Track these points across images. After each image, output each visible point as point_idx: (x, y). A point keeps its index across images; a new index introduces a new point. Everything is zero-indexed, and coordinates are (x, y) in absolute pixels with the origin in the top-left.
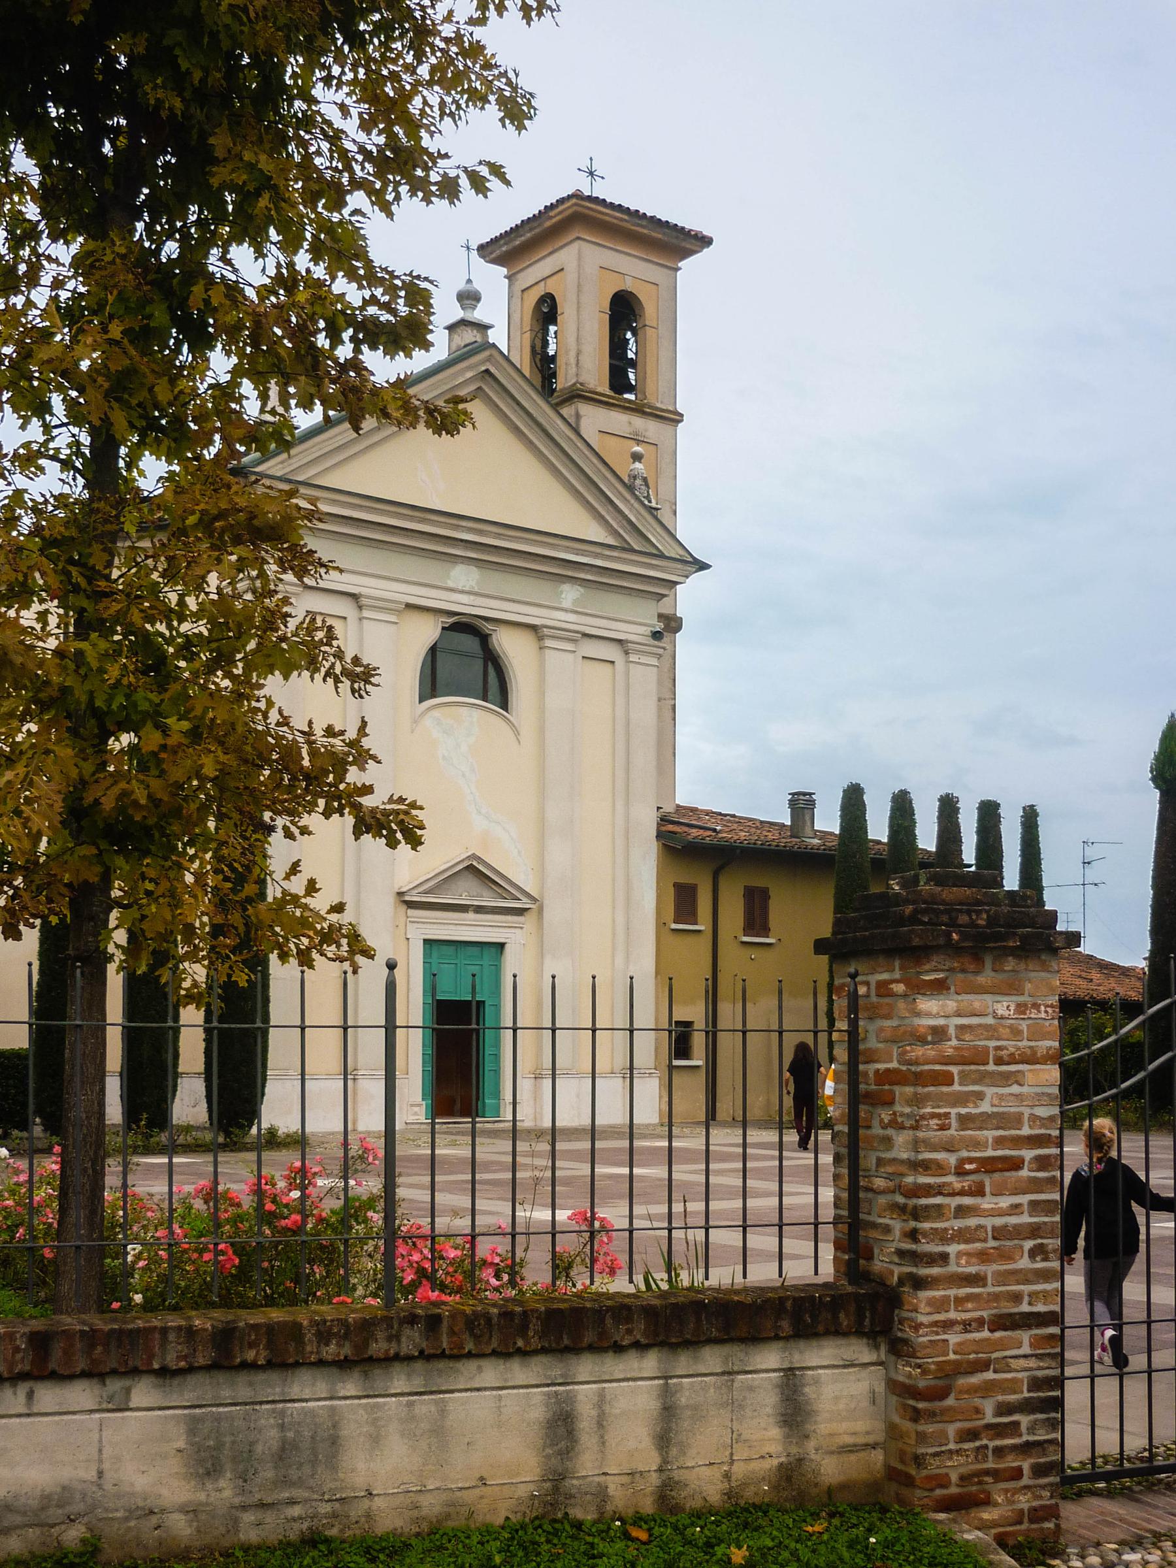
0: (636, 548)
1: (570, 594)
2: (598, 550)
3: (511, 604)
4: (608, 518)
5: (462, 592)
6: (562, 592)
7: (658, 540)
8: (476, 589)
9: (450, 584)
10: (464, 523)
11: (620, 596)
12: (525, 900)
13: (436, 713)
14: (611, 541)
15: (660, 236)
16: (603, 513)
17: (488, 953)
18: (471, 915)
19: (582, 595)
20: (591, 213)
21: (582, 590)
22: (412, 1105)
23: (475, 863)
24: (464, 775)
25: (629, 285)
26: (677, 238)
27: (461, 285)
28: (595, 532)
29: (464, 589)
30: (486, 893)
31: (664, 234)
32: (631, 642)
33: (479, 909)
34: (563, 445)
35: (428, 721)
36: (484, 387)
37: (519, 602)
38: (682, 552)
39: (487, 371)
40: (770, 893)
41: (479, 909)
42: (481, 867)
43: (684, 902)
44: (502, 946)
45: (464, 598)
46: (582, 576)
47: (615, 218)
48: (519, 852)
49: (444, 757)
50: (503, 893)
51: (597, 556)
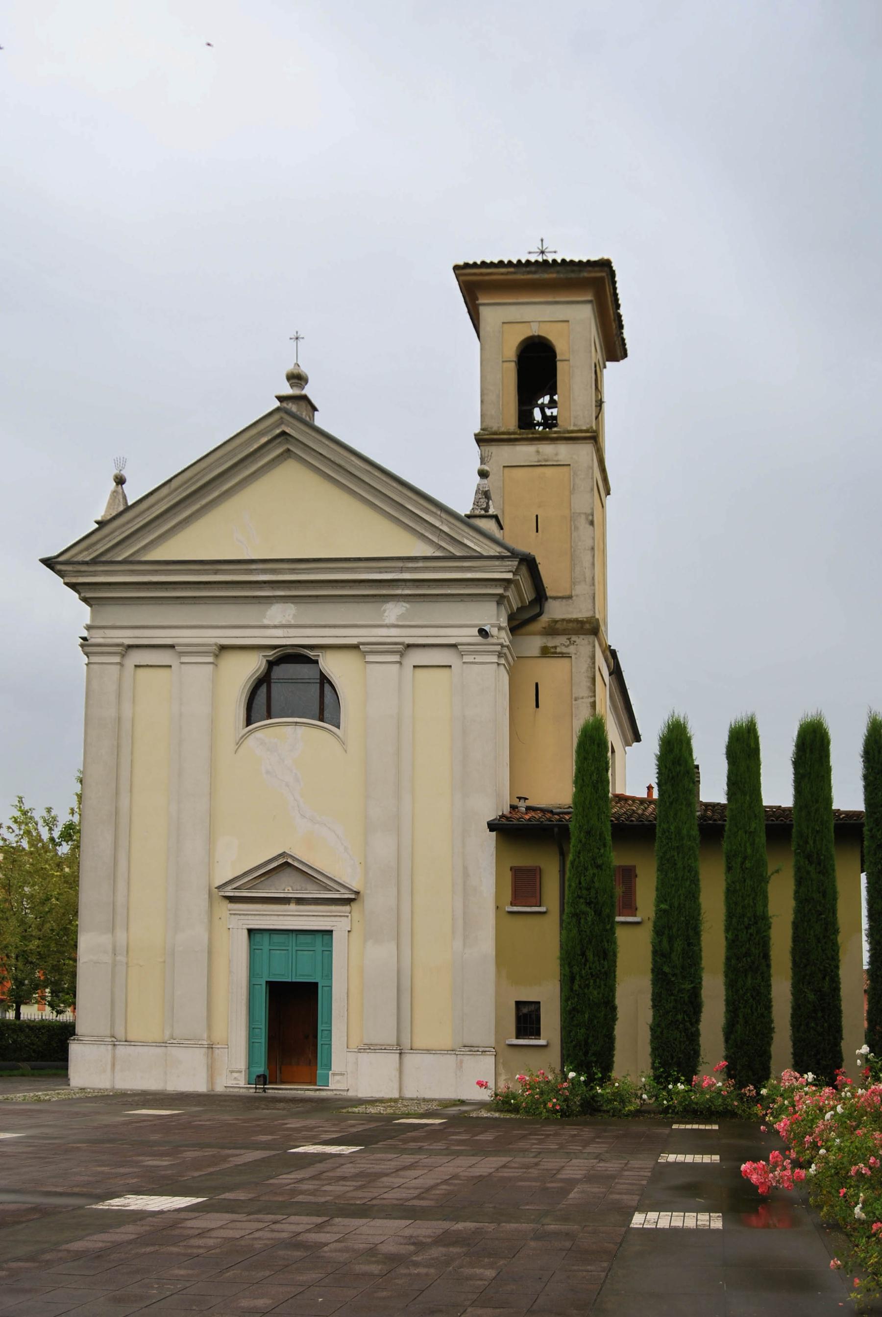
0: (458, 554)
1: (393, 612)
2: (400, 564)
3: (327, 630)
4: (427, 534)
5: (275, 627)
6: (385, 611)
7: (475, 544)
8: (293, 622)
9: (266, 622)
10: (254, 567)
11: (447, 604)
12: (343, 891)
13: (258, 734)
14: (438, 554)
15: (554, 276)
16: (423, 532)
17: (319, 939)
18: (293, 907)
19: (407, 609)
20: (487, 278)
21: (407, 605)
22: (232, 1072)
23: (290, 861)
24: (287, 785)
25: (535, 330)
26: (573, 271)
27: (290, 367)
28: (422, 549)
29: (282, 624)
30: (310, 886)
31: (558, 272)
32: (363, 644)
33: (300, 901)
34: (367, 480)
35: (251, 741)
36: (292, 448)
37: (335, 626)
38: (499, 549)
39: (284, 433)
40: (638, 872)
41: (300, 901)
42: (296, 864)
43: (523, 887)
44: (330, 932)
45: (279, 632)
46: (399, 592)
47: (502, 274)
48: (346, 849)
49: (268, 772)
50: (327, 888)
51: (402, 570)
